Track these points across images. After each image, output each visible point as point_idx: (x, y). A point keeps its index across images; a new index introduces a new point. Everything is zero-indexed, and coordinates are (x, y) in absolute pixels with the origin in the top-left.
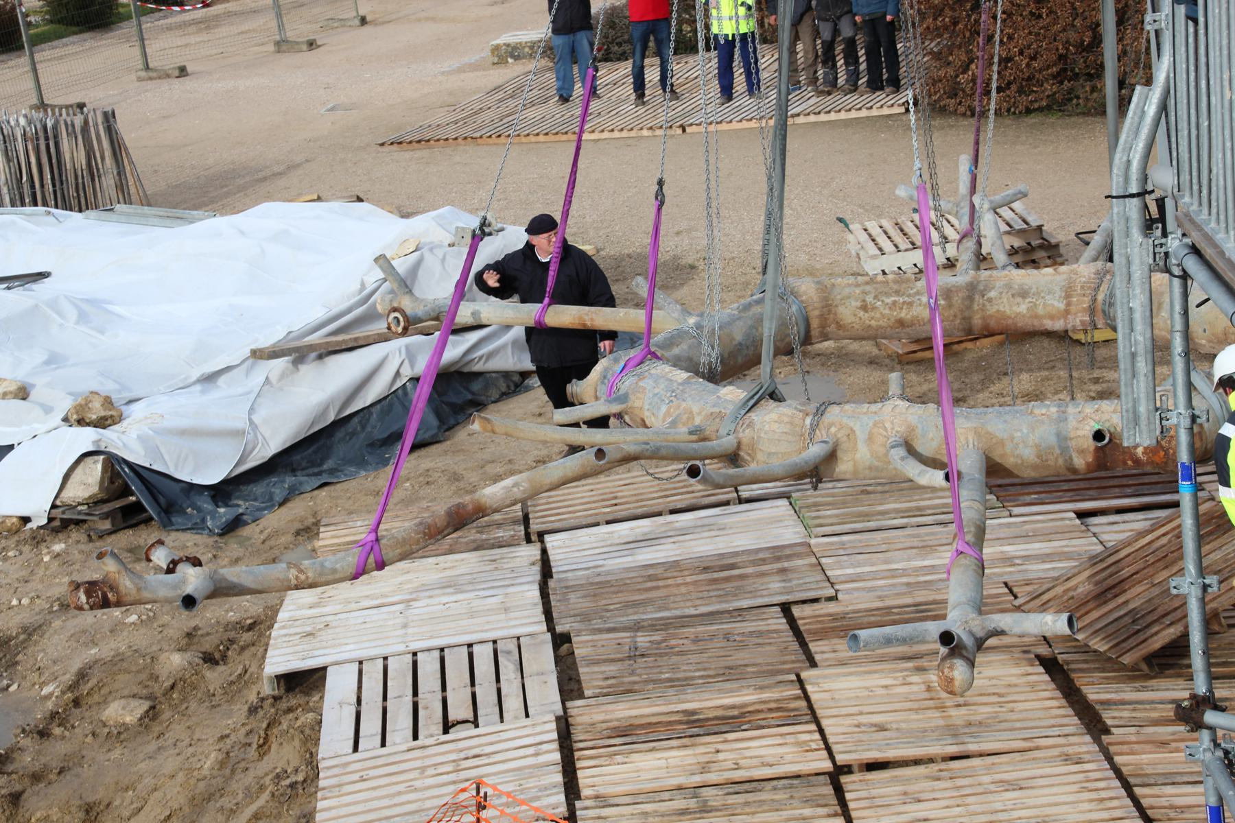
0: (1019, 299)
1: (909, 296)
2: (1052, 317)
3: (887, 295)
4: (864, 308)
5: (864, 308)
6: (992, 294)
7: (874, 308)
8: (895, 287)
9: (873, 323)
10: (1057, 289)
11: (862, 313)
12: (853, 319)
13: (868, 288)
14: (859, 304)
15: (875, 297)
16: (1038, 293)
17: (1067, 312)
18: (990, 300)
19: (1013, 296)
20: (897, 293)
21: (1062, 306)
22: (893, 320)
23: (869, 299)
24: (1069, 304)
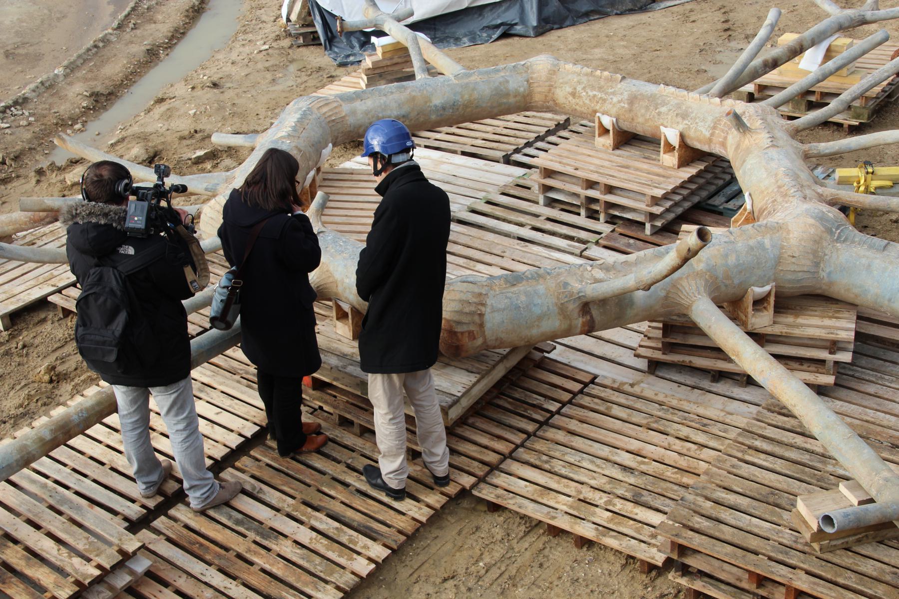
0: (679, 119)
1: (606, 94)
2: (700, 141)
3: (593, 88)
4: (573, 94)
5: (573, 94)
6: (663, 109)
8: (602, 83)
9: (577, 107)
10: (710, 118)
11: (570, 98)
13: (584, 79)
14: (570, 90)
15: (584, 88)
16: (695, 119)
17: (710, 141)
18: (659, 114)
19: (677, 115)
20: (600, 89)
21: (707, 134)
22: (591, 110)
23: (579, 88)
24: (712, 135)
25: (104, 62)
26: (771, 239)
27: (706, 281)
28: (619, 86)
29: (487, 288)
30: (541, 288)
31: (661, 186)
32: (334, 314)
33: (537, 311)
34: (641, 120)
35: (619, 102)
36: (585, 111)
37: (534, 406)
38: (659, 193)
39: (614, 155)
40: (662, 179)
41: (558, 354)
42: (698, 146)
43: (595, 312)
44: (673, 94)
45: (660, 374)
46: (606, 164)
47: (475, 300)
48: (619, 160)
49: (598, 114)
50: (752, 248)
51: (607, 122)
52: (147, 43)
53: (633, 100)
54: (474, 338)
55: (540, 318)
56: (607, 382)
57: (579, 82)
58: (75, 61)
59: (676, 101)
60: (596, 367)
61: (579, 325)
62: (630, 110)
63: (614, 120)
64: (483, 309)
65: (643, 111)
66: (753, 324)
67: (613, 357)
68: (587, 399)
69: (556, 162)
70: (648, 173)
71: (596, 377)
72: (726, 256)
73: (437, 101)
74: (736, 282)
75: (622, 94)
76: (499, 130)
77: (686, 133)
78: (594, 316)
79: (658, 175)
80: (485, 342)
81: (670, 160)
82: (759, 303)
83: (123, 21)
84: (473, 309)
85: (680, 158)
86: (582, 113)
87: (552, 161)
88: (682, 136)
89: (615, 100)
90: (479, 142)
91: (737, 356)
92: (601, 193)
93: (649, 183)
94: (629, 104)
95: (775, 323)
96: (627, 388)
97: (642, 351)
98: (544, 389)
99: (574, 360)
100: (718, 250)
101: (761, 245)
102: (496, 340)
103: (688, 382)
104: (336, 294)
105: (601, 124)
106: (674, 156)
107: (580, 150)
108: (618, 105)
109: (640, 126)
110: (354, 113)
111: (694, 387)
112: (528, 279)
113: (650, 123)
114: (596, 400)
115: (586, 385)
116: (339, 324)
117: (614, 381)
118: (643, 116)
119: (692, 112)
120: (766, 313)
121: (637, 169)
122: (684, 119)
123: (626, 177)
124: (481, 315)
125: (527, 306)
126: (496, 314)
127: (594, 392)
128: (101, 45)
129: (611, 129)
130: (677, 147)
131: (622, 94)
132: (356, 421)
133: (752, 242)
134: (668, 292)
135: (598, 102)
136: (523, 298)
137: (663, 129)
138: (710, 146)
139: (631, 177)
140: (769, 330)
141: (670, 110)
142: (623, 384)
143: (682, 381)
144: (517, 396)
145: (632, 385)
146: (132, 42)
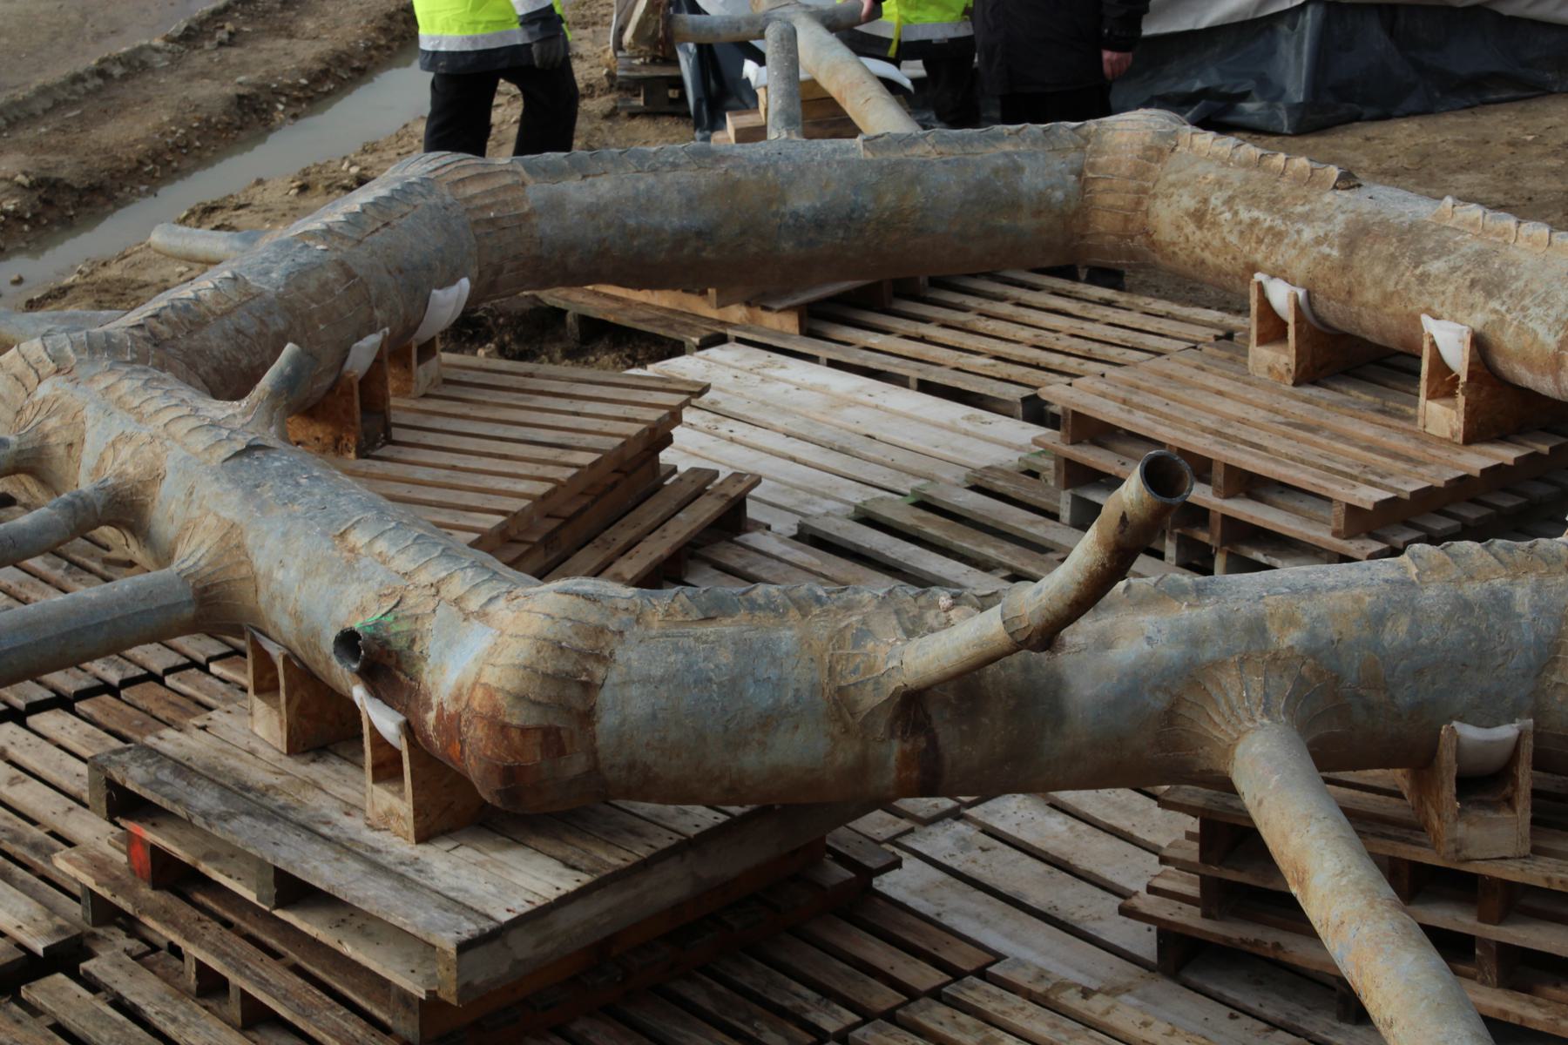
0: (1478, 296)
1: (1287, 217)
2: (1529, 363)
3: (1253, 199)
5: (1199, 217)
6: (1436, 267)
7: (1214, 224)
8: (1283, 188)
9: (1207, 255)
11: (1190, 227)
12: (1175, 234)
13: (1236, 176)
15: (1229, 201)
16: (1523, 295)
18: (1423, 279)
19: (1473, 283)
20: (1273, 204)
22: (1241, 261)
23: (1216, 201)
25: (105, 114)
26: (1537, 590)
27: (1300, 680)
28: (1329, 197)
29: (625, 617)
30: (787, 636)
31: (1387, 481)
32: (247, 680)
33: (763, 699)
34: (1371, 295)
35: (1318, 241)
36: (1227, 267)
37: (782, 1013)
38: (1368, 497)
39: (1296, 398)
40: (1400, 465)
41: (904, 883)
42: (1527, 378)
43: (948, 736)
44: (1473, 224)
45: (1195, 979)
46: (1256, 415)
47: (579, 643)
48: (1299, 410)
49: (1258, 277)
50: (1466, 606)
51: (1282, 296)
52: (243, 81)
53: (1356, 236)
54: (561, 752)
55: (769, 721)
56: (1020, 978)
57: (1220, 184)
58: (26, 101)
59: (1477, 245)
60: (1010, 936)
61: (893, 762)
62: (1345, 268)
63: (1301, 293)
64: (600, 672)
65: (1379, 270)
66: (1460, 845)
67: (1075, 916)
68: (941, 1011)
69: (1114, 399)
70: (1369, 449)
71: (999, 957)
72: (1378, 619)
73: (802, 202)
74: (1404, 699)
75: (1329, 220)
76: (1049, 339)
77: (1495, 337)
78: (942, 741)
79: (1395, 455)
80: (594, 769)
81: (1443, 417)
82: (1483, 783)
83: (202, 23)
84: (569, 667)
85: (1471, 415)
86: (1219, 272)
87: (1103, 395)
88: (1480, 345)
89: (1308, 235)
90: (978, 362)
91: (1301, 883)
92: (1216, 493)
93: (1355, 472)
94: (1342, 247)
95: (1537, 851)
96: (1072, 1000)
97: (1146, 903)
98: (835, 974)
99: (956, 911)
100: (1357, 600)
101: (1501, 603)
102: (631, 766)
103: (1269, 1012)
104: (255, 614)
105: (1265, 303)
106: (1455, 407)
107: (1211, 381)
108: (1314, 252)
109: (1371, 307)
110: (555, 206)
111: (1274, 1026)
112: (753, 606)
113: (1396, 306)
114: (963, 1018)
115: (957, 975)
116: (259, 705)
117: (1042, 975)
118: (1378, 283)
119: (1516, 278)
120: (1505, 815)
121: (1339, 436)
122: (1489, 295)
123: (1293, 452)
124: (589, 687)
125: (733, 681)
126: (634, 691)
127: (970, 997)
128: (117, 71)
129: (1290, 319)
130: (1463, 378)
131: (1329, 220)
132: (235, 980)
133: (1472, 590)
134: (1177, 701)
135: (1260, 241)
136: (725, 657)
137: (1428, 323)
138: (1557, 381)
139: (1310, 453)
140: (1513, 872)
141: (1454, 270)
142: (1063, 986)
143: (1252, 1004)
144: (746, 980)
145: (1086, 993)
146: (205, 75)
